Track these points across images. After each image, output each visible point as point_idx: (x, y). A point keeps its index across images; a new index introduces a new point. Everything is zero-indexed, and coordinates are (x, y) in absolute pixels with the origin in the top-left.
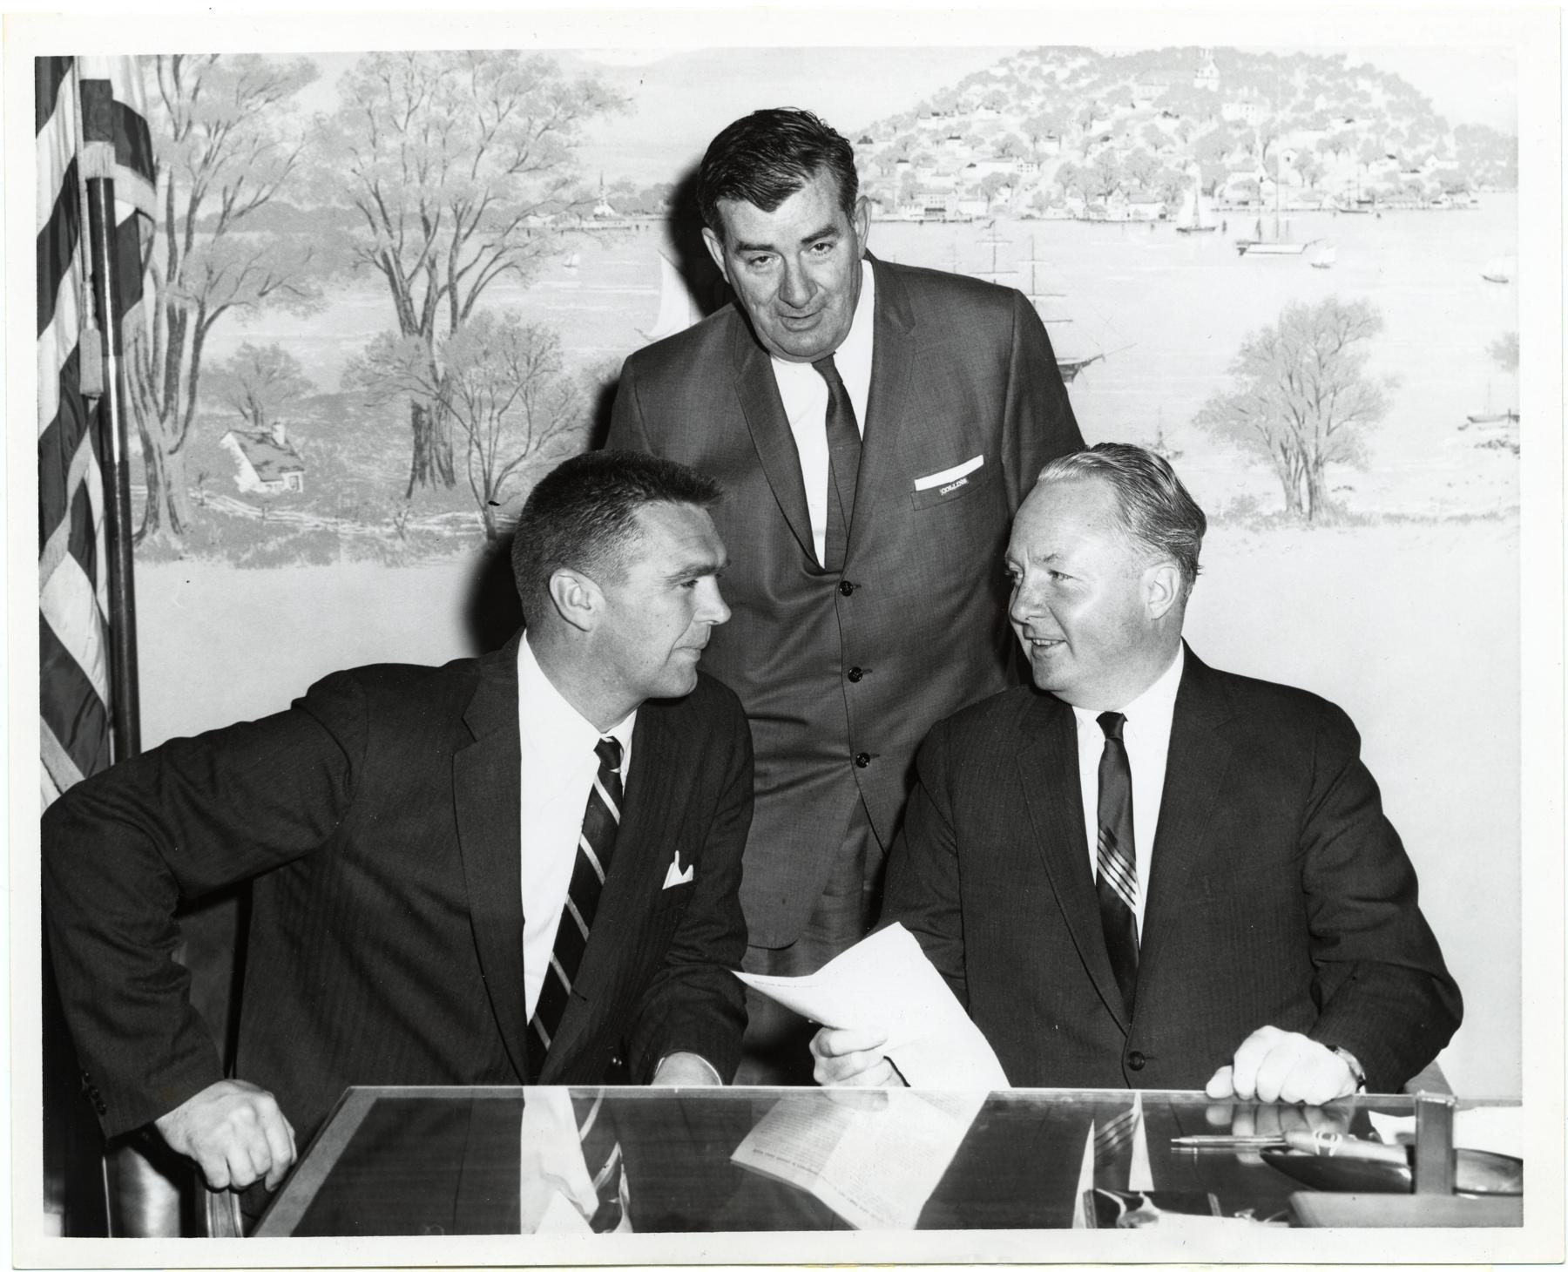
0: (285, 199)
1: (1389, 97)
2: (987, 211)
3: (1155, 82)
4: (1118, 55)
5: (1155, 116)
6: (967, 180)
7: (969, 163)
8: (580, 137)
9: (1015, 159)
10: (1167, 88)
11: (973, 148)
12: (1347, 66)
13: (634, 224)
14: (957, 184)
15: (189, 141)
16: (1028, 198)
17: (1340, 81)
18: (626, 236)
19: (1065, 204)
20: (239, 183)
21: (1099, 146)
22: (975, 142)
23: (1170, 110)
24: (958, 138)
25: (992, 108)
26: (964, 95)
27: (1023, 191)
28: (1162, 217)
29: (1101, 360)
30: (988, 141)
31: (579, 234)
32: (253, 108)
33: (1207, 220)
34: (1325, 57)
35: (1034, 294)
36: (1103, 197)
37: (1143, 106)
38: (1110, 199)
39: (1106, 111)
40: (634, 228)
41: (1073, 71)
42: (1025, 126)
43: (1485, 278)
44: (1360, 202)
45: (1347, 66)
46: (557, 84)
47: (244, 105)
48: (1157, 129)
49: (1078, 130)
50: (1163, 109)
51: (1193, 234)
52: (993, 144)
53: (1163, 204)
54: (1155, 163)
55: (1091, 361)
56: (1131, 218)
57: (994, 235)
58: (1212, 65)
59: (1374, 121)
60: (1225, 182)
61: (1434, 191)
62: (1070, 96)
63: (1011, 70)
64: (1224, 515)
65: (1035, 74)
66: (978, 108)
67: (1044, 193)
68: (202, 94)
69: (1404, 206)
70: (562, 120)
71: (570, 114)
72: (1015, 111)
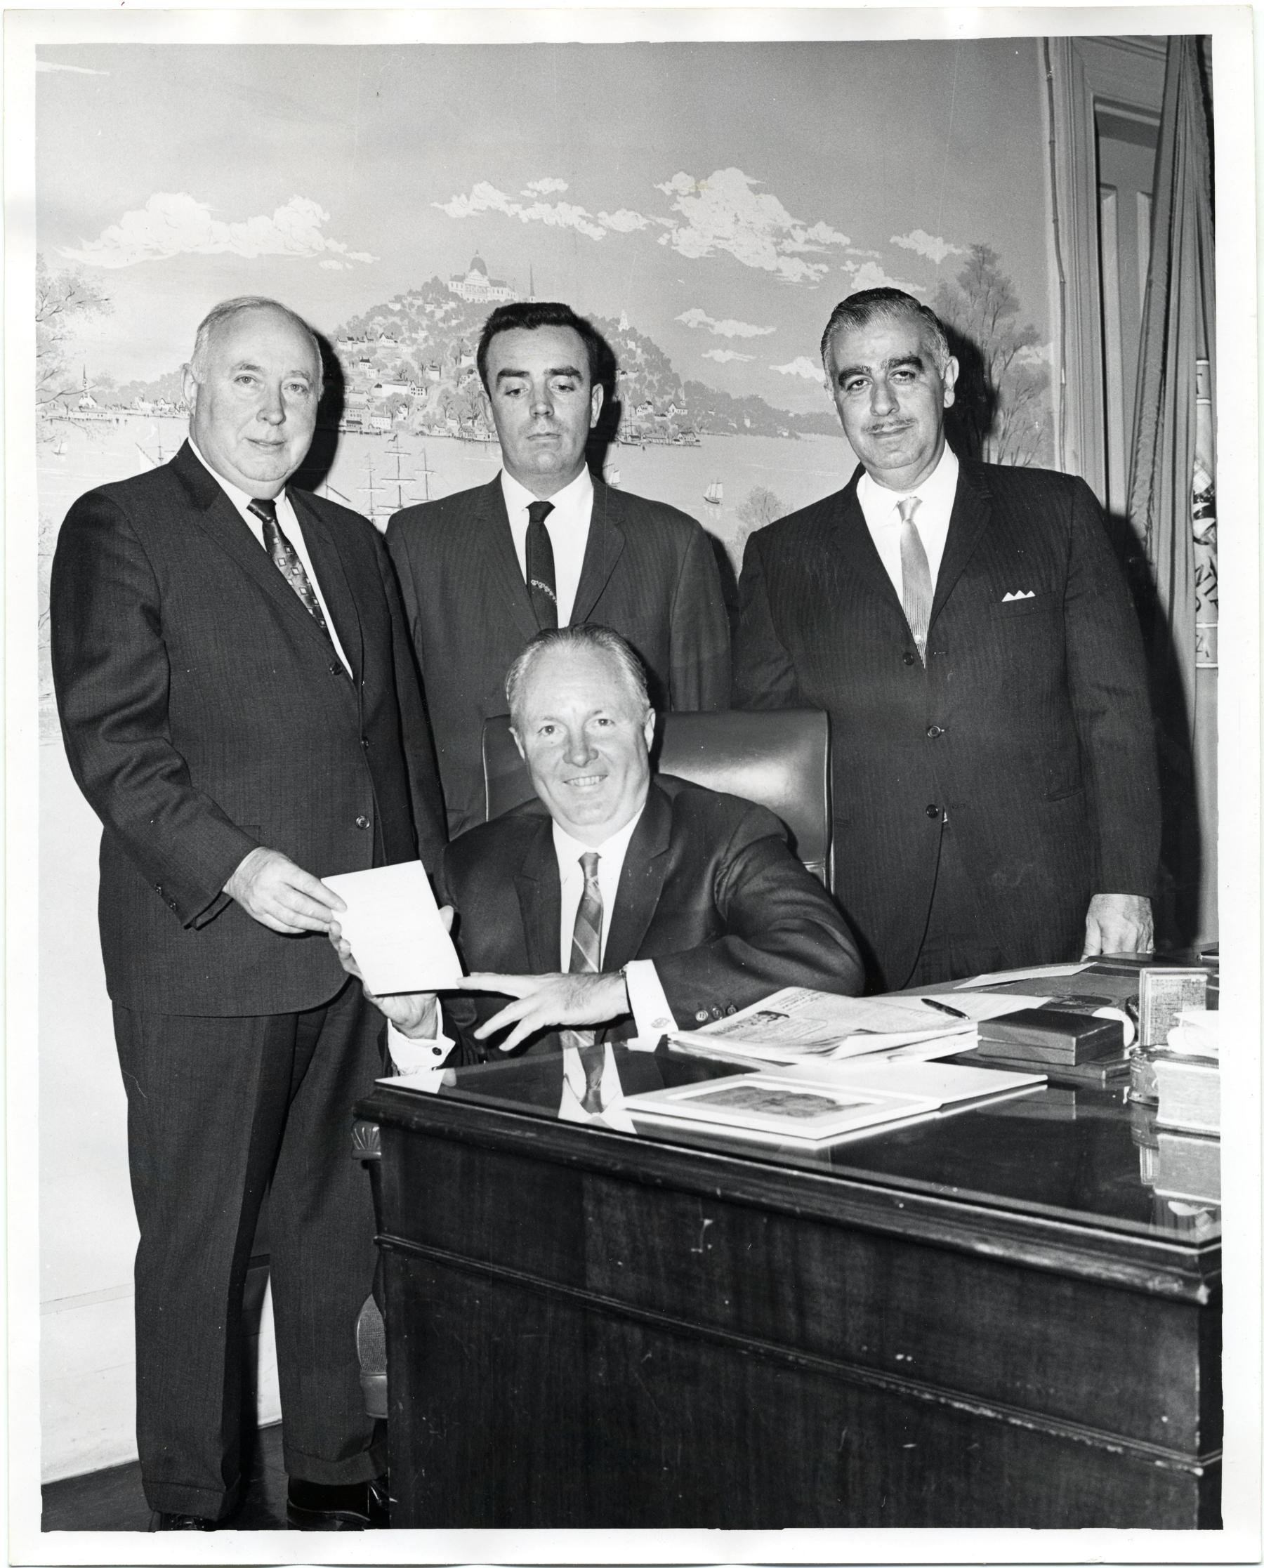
1: (645, 356)
4: (476, 302)
6: (377, 398)
7: (376, 384)
8: (64, 331)
11: (379, 371)
12: (620, 329)
13: (114, 418)
16: (419, 418)
17: (617, 340)
18: (108, 428)
19: (446, 424)
22: (380, 367)
24: (368, 361)
25: (391, 338)
26: (370, 323)
30: (390, 365)
31: (66, 423)
34: (607, 320)
38: (476, 424)
40: (115, 421)
41: (446, 312)
42: (413, 355)
43: (707, 500)
44: (632, 437)
45: (620, 329)
46: (43, 278)
49: (452, 363)
52: (392, 369)
59: (638, 374)
61: (674, 429)
65: (421, 310)
67: (431, 413)
69: (658, 441)
70: (48, 313)
71: (55, 308)
72: (407, 342)
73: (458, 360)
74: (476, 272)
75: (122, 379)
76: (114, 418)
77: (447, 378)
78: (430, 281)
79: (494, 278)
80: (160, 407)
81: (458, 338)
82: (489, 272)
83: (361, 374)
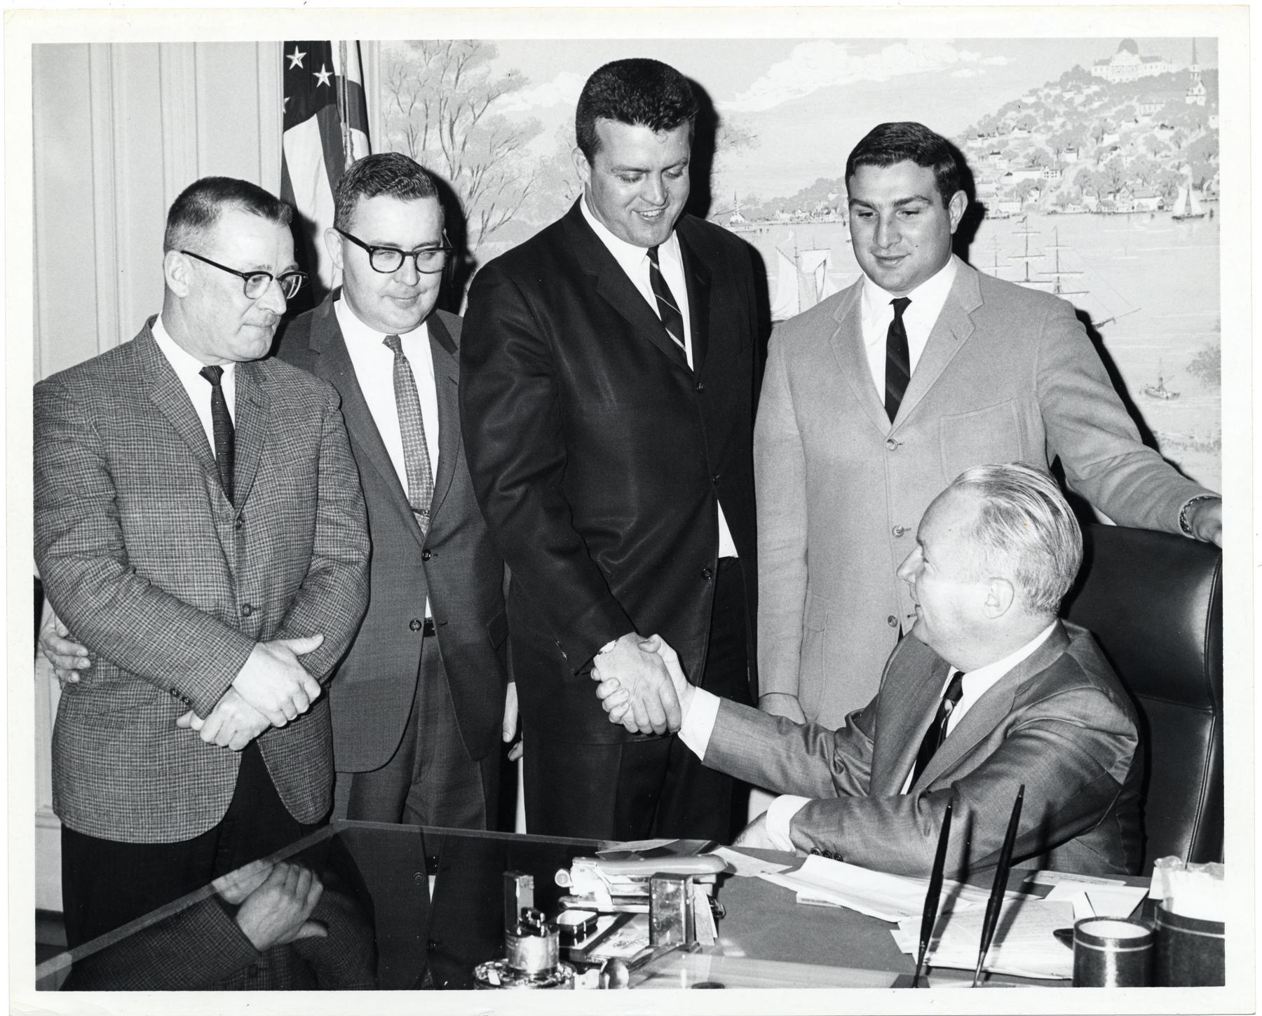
0: (522, 219)
2: (1021, 209)
3: (1154, 101)
4: (1124, 81)
5: (1154, 128)
6: (1005, 185)
7: (1006, 173)
9: (1043, 168)
10: (1163, 105)
11: (1010, 160)
14: (997, 189)
15: (460, 179)
16: (1052, 198)
19: (1082, 201)
20: (492, 208)
21: (1109, 154)
22: (1011, 157)
23: (1166, 124)
24: (999, 153)
25: (1024, 129)
26: (1003, 120)
27: (1051, 194)
28: (1160, 208)
29: (1111, 322)
30: (1021, 155)
32: (501, 155)
33: (1197, 209)
35: (1058, 272)
36: (1112, 195)
37: (1144, 121)
38: (1118, 196)
39: (1114, 126)
40: (758, 231)
42: (1048, 141)
47: (495, 153)
48: (1156, 138)
49: (1092, 143)
50: (1160, 123)
51: (1186, 220)
52: (1025, 157)
53: (1161, 198)
54: (1155, 166)
55: (1104, 323)
56: (1135, 210)
57: (1026, 228)
58: (1200, 84)
60: (1213, 178)
62: (1085, 116)
63: (1040, 98)
64: (1214, 443)
65: (1059, 99)
66: (1013, 129)
67: (1066, 194)
68: (466, 146)
72: (1042, 130)
73: (1099, 139)
74: (1125, 52)
75: (767, 197)
76: (758, 228)
77: (1086, 157)
78: (1070, 70)
79: (1148, 55)
80: (797, 215)
81: (1100, 119)
82: (1141, 50)
83: (990, 166)
